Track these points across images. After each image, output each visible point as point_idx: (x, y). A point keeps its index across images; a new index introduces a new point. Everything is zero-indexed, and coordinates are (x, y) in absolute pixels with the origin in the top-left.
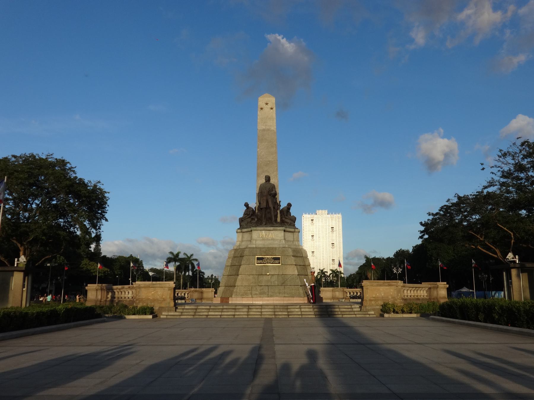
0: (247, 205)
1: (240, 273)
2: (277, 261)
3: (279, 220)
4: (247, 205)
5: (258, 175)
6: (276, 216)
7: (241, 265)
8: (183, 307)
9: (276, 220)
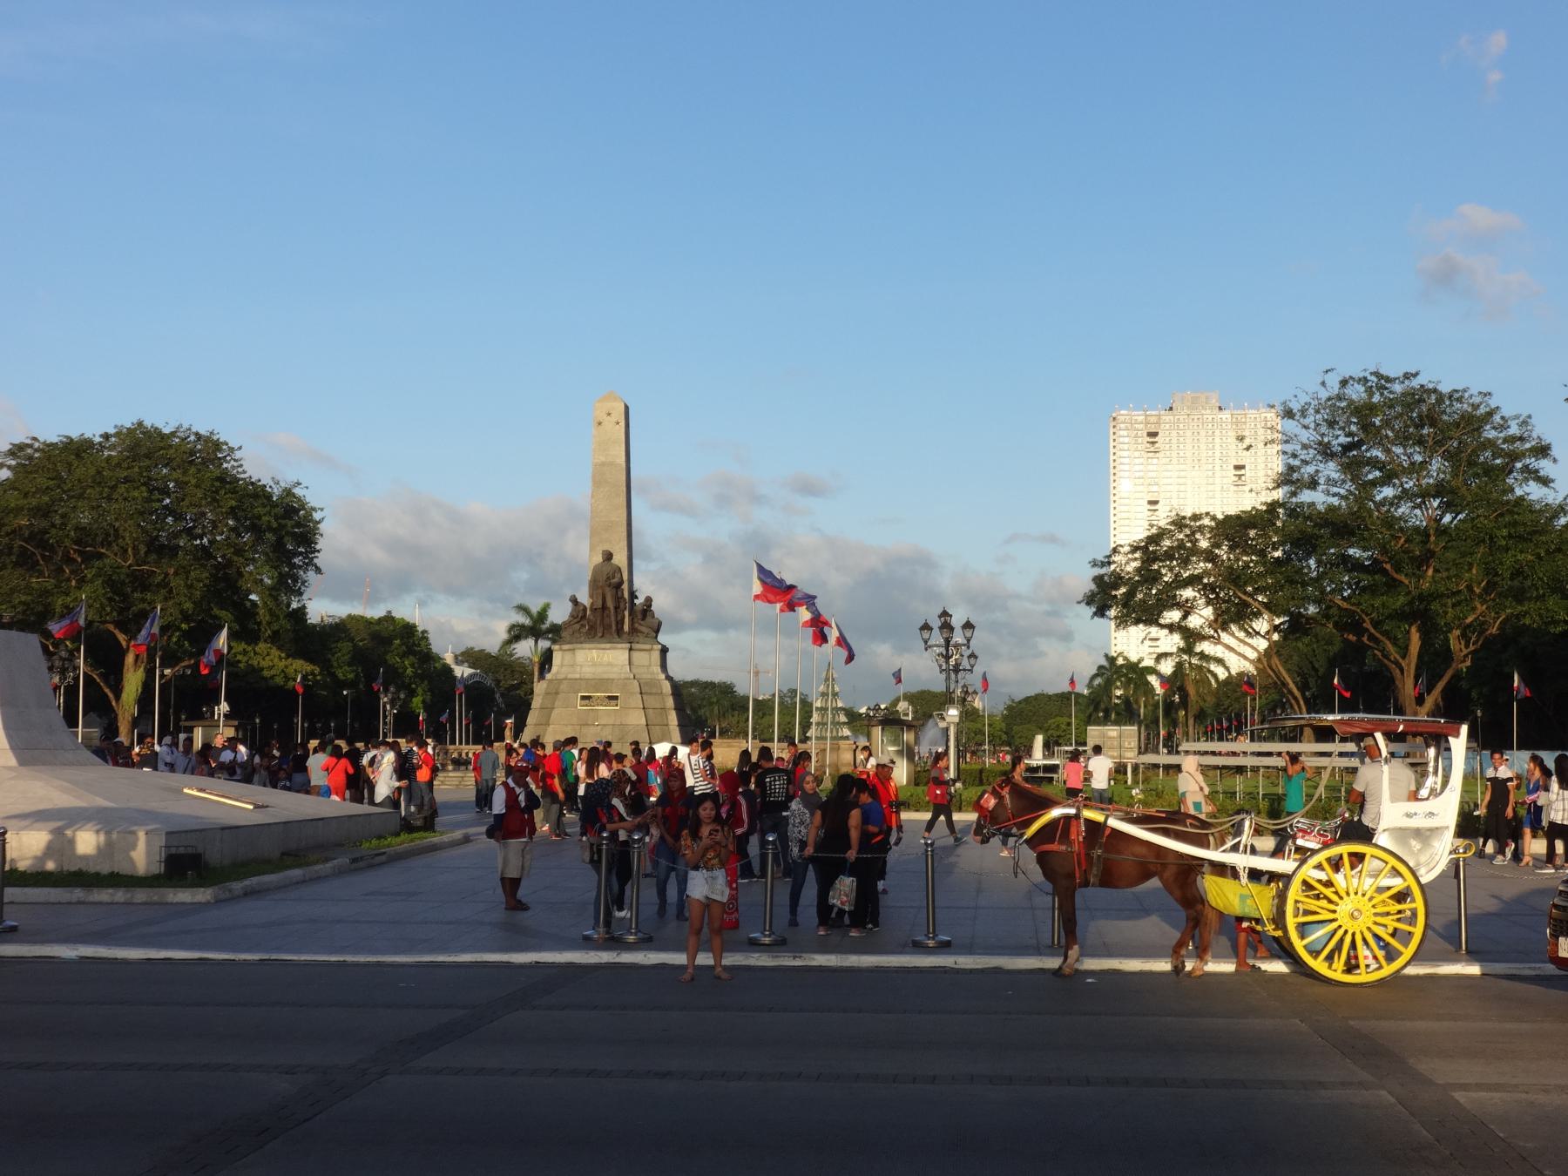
0: (574, 601)
1: (551, 722)
2: (614, 702)
3: (626, 628)
4: (574, 601)
5: (592, 548)
6: (620, 623)
7: (553, 708)
8: (446, 775)
9: (619, 631)
